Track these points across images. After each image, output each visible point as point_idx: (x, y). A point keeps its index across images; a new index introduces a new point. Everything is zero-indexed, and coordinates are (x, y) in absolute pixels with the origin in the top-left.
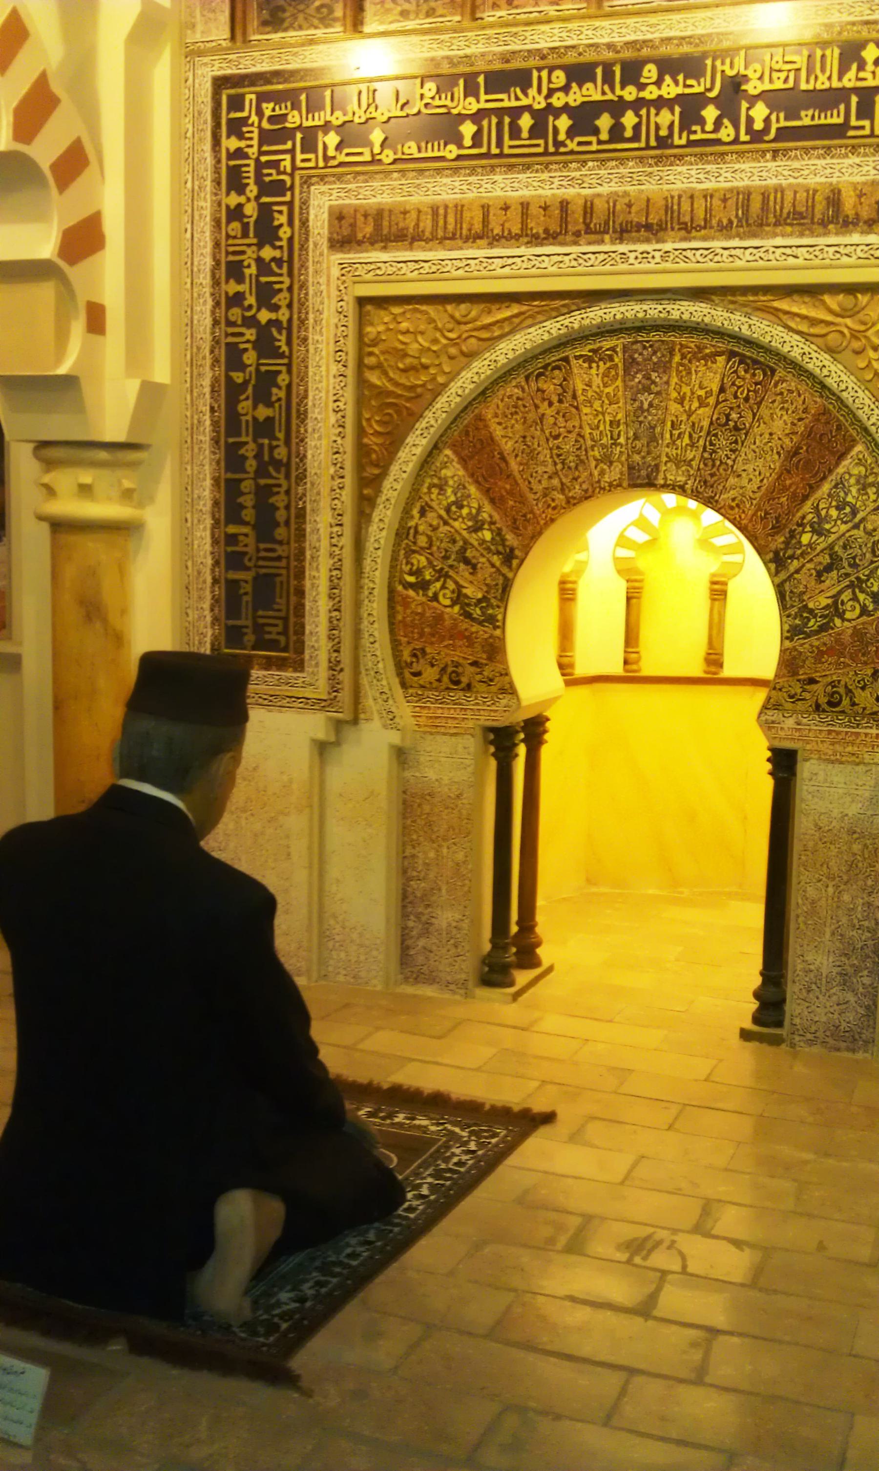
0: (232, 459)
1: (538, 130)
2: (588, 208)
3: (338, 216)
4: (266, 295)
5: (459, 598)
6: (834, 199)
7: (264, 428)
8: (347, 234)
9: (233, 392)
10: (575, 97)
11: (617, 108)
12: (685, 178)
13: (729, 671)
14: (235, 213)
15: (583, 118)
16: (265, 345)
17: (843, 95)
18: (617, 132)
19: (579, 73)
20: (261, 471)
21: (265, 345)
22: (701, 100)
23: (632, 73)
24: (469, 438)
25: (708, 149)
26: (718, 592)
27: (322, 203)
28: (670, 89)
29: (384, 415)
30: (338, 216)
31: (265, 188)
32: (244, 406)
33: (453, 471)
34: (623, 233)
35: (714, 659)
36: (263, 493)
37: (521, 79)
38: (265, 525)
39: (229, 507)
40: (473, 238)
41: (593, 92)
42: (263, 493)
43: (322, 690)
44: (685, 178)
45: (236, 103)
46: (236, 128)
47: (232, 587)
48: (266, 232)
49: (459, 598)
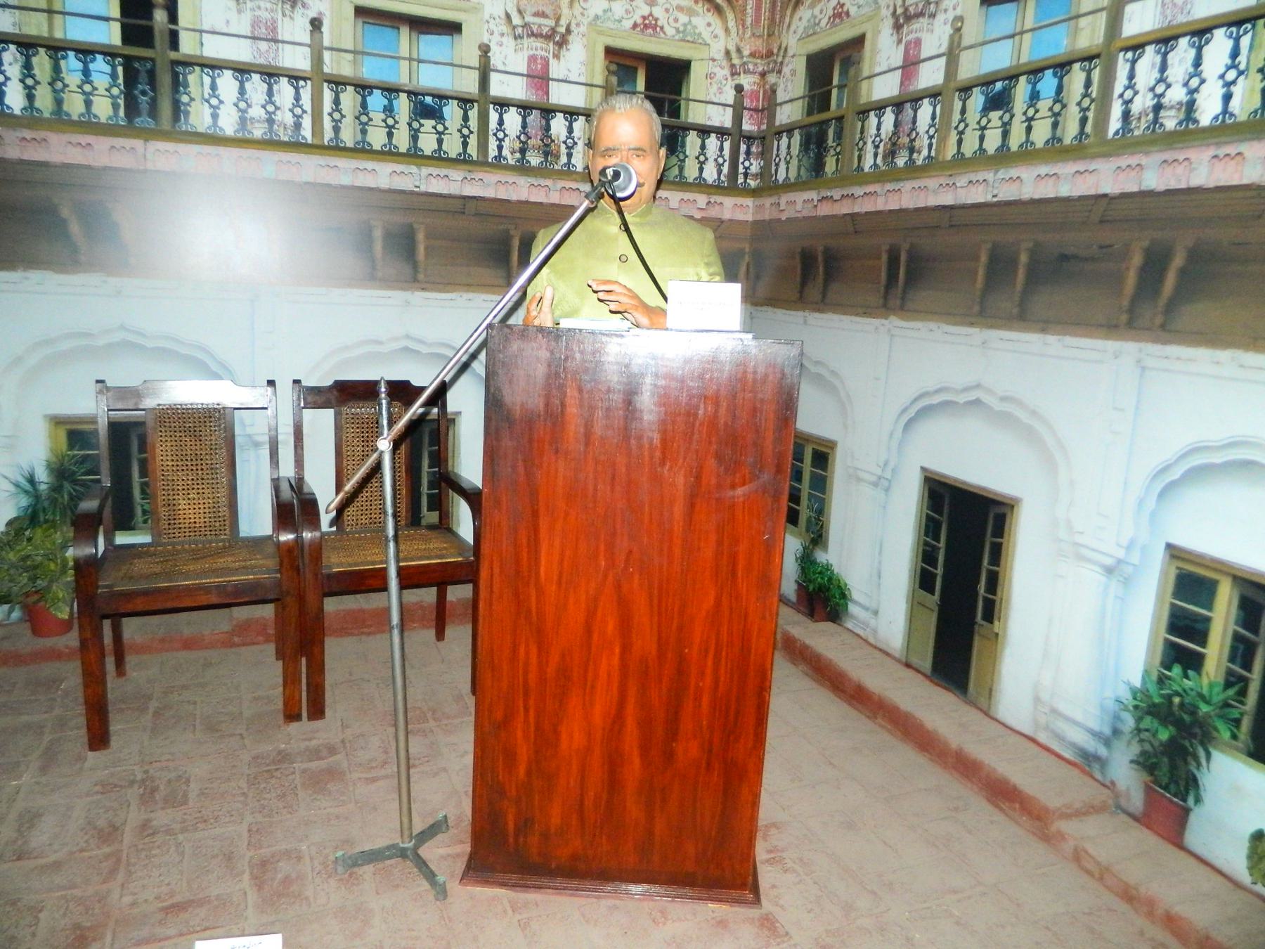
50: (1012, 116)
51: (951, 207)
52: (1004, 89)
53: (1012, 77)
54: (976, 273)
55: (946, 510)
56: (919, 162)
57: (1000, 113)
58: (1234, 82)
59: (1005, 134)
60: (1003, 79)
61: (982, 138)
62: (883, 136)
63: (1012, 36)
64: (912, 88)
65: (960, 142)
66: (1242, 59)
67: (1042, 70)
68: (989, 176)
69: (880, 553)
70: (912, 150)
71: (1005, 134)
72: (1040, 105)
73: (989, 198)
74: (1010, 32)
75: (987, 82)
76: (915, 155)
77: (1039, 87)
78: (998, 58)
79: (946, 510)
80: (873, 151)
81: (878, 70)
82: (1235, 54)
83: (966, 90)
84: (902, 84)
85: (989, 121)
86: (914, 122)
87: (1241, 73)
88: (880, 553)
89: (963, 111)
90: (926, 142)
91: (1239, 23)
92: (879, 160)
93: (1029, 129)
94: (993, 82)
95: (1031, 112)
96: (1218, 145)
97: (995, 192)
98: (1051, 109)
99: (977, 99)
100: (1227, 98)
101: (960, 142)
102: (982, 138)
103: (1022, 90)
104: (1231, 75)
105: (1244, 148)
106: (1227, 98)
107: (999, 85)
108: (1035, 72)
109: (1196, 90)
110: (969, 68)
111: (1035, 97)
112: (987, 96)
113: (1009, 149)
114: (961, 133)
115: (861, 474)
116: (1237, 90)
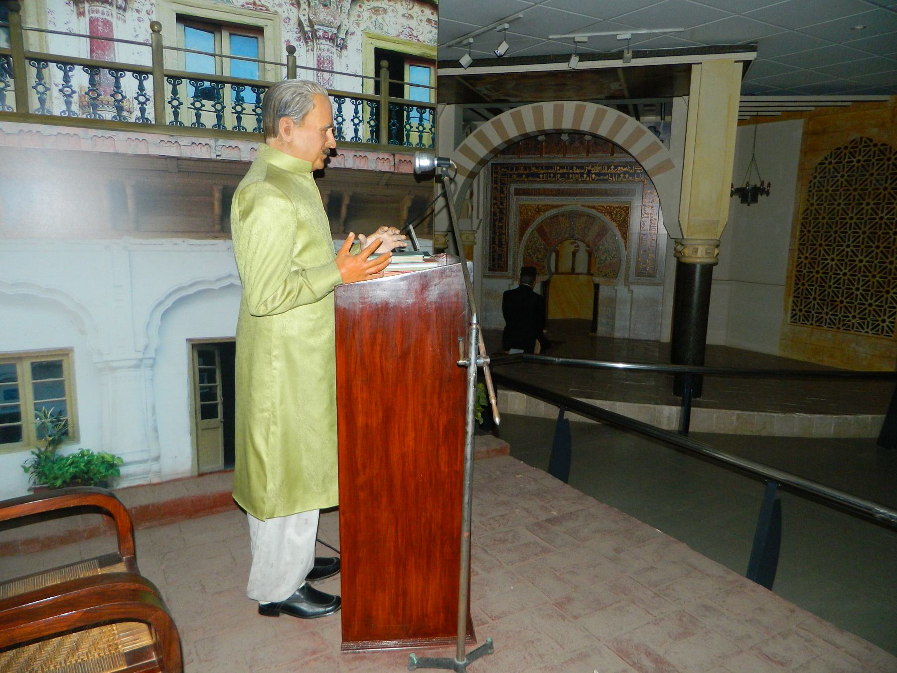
0: (494, 233)
1: (554, 177)
2: (563, 190)
3: (516, 189)
4: (502, 203)
5: (537, 258)
6: (606, 190)
7: (501, 227)
8: (518, 192)
9: (495, 220)
10: (561, 171)
11: (569, 174)
12: (580, 186)
13: (576, 271)
14: (496, 188)
15: (563, 175)
16: (501, 212)
17: (607, 174)
18: (568, 178)
19: (562, 167)
20: (500, 234)
21: (501, 212)
22: (583, 173)
23: (571, 168)
24: (540, 230)
25: (584, 182)
26: (574, 254)
27: (513, 187)
28: (578, 171)
29: (524, 225)
30: (516, 189)
31: (502, 184)
32: (497, 223)
33: (536, 235)
34: (570, 195)
35: (573, 269)
36: (500, 240)
37: (552, 168)
38: (500, 245)
39: (493, 241)
40: (542, 195)
41: (564, 171)
42: (500, 240)
43: (511, 274)
44: (580, 186)
45: (496, 168)
46: (496, 173)
47: (493, 257)
48: (502, 192)
49: (537, 258)
50: (223, 108)
51: (178, 158)
52: (213, 88)
53: (220, 82)
54: (212, 204)
55: (217, 360)
56: (133, 120)
57: (213, 103)
58: (358, 124)
59: (220, 117)
60: (211, 81)
61: (198, 116)
62: (75, 88)
63: (214, 55)
64: (107, 59)
65: (176, 114)
66: (360, 114)
67: (244, 85)
68: (212, 142)
69: (154, 413)
70: (120, 109)
71: (220, 117)
72: (244, 106)
73: (214, 156)
74: (212, 52)
75: (195, 79)
76: (125, 113)
77: (242, 94)
78: (206, 66)
79: (217, 360)
80: (63, 99)
81: (51, 27)
82: (356, 112)
83: (175, 78)
84: (92, 51)
85: (203, 105)
86: (117, 85)
87: (360, 121)
88: (154, 413)
89: (175, 92)
90: (137, 106)
91: (357, 99)
92: (75, 108)
93: (239, 119)
94: (202, 80)
95: (239, 108)
96: (356, 151)
97: (218, 153)
98: (254, 110)
99: (187, 90)
100: (356, 131)
101: (176, 114)
102: (198, 116)
103: (228, 93)
104: (356, 121)
105: (367, 154)
106: (356, 131)
107: (207, 84)
108: (238, 85)
109: (341, 123)
110: (172, 62)
111: (239, 100)
112: (197, 88)
113: (224, 127)
114: (176, 108)
115: (114, 364)
116: (360, 128)
